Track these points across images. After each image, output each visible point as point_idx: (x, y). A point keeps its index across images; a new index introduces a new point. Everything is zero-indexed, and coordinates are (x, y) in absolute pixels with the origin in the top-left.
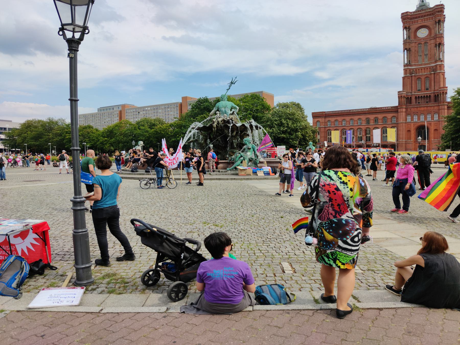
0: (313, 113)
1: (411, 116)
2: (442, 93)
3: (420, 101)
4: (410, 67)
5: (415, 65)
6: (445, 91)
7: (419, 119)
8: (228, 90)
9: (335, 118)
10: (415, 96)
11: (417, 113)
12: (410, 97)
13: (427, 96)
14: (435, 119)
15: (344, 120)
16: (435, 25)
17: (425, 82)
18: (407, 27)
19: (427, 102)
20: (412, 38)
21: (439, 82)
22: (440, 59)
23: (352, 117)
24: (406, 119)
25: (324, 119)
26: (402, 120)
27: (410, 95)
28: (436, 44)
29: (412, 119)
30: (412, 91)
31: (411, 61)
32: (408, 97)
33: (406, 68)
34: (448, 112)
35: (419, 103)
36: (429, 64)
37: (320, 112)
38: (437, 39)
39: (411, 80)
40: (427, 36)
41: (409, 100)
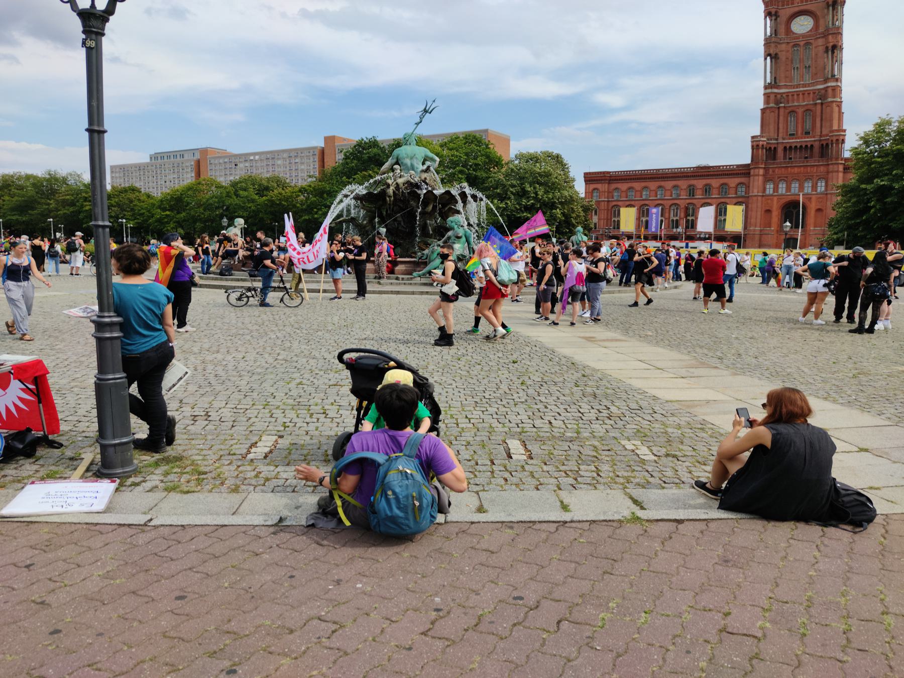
0: (586, 174)
1: (774, 184)
2: (834, 141)
3: (792, 156)
4: (776, 91)
5: (786, 87)
6: (841, 138)
7: (788, 189)
8: (417, 124)
9: (630, 185)
10: (785, 145)
11: (787, 177)
12: (775, 148)
13: (806, 146)
14: (819, 189)
15: (646, 187)
16: (826, 11)
17: (803, 118)
18: (773, 13)
19: (806, 158)
20: (782, 35)
21: (831, 120)
22: (833, 76)
23: (662, 183)
24: (765, 189)
25: (607, 185)
26: (755, 191)
27: (774, 143)
28: (827, 48)
29: (776, 189)
30: (778, 136)
31: (778, 78)
32: (770, 148)
33: (769, 91)
34: (844, 178)
35: (790, 159)
36: (813, 84)
37: (601, 173)
38: (830, 37)
39: (777, 115)
40: (811, 31)
41: (771, 153)
